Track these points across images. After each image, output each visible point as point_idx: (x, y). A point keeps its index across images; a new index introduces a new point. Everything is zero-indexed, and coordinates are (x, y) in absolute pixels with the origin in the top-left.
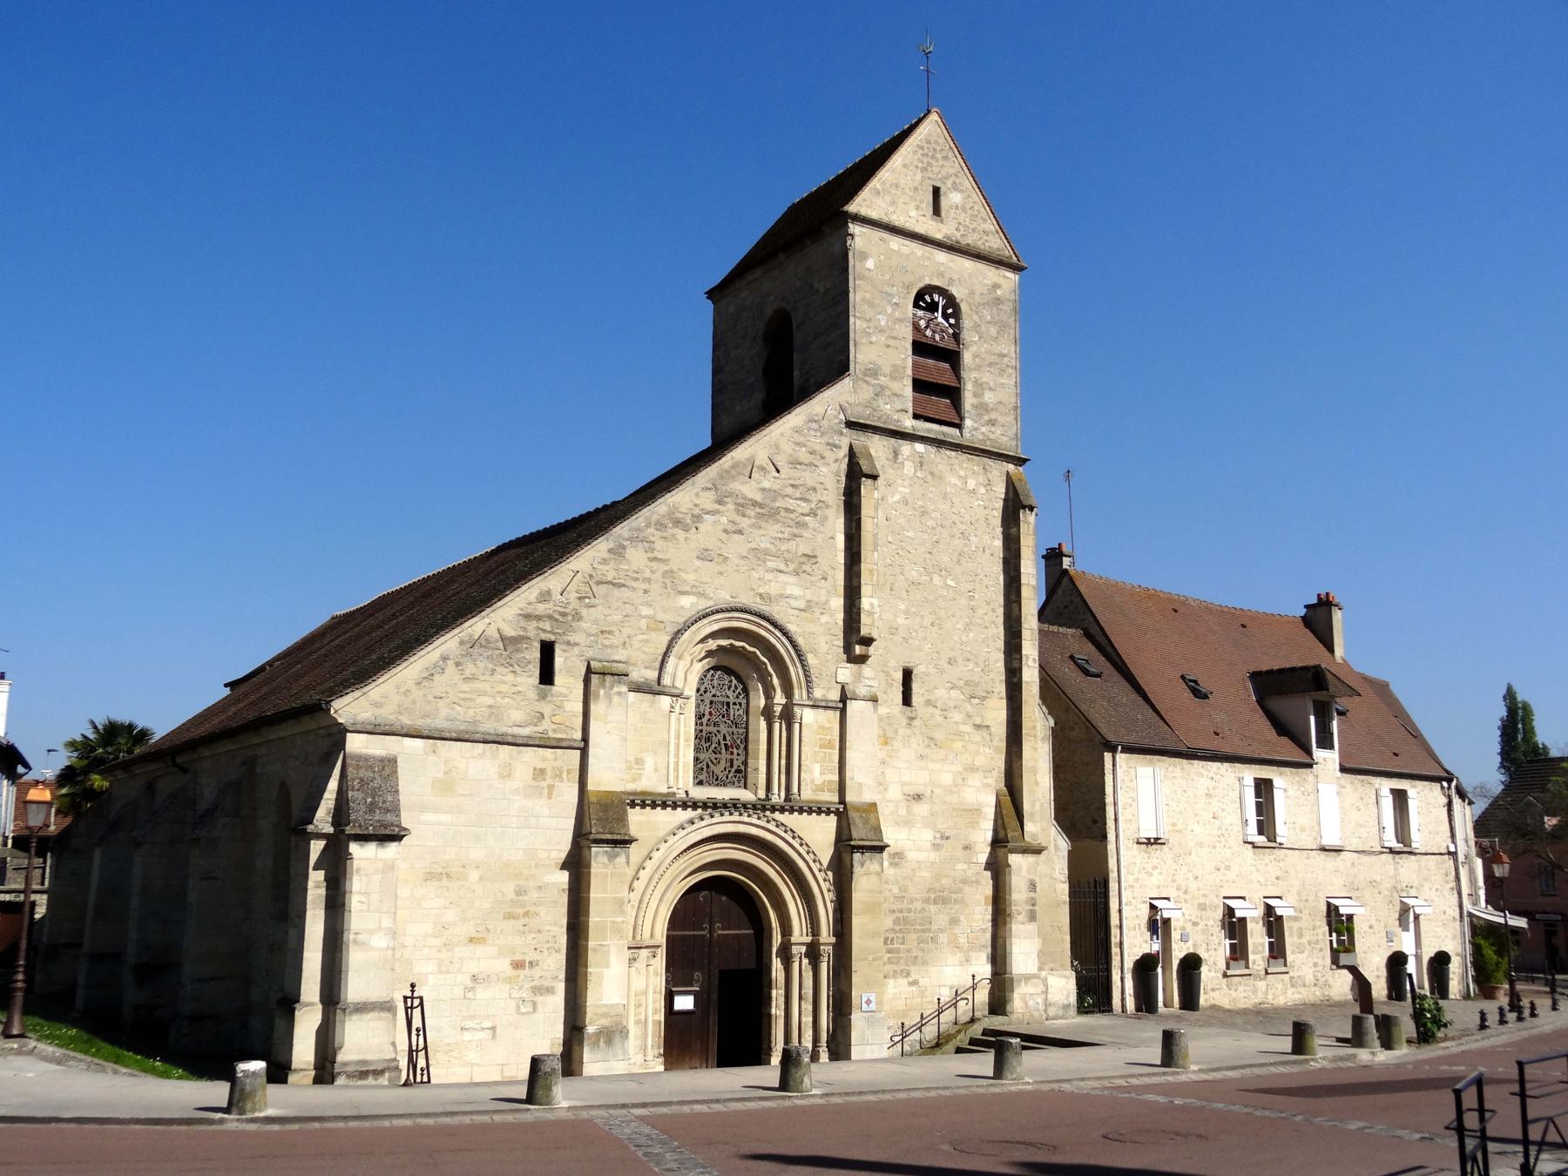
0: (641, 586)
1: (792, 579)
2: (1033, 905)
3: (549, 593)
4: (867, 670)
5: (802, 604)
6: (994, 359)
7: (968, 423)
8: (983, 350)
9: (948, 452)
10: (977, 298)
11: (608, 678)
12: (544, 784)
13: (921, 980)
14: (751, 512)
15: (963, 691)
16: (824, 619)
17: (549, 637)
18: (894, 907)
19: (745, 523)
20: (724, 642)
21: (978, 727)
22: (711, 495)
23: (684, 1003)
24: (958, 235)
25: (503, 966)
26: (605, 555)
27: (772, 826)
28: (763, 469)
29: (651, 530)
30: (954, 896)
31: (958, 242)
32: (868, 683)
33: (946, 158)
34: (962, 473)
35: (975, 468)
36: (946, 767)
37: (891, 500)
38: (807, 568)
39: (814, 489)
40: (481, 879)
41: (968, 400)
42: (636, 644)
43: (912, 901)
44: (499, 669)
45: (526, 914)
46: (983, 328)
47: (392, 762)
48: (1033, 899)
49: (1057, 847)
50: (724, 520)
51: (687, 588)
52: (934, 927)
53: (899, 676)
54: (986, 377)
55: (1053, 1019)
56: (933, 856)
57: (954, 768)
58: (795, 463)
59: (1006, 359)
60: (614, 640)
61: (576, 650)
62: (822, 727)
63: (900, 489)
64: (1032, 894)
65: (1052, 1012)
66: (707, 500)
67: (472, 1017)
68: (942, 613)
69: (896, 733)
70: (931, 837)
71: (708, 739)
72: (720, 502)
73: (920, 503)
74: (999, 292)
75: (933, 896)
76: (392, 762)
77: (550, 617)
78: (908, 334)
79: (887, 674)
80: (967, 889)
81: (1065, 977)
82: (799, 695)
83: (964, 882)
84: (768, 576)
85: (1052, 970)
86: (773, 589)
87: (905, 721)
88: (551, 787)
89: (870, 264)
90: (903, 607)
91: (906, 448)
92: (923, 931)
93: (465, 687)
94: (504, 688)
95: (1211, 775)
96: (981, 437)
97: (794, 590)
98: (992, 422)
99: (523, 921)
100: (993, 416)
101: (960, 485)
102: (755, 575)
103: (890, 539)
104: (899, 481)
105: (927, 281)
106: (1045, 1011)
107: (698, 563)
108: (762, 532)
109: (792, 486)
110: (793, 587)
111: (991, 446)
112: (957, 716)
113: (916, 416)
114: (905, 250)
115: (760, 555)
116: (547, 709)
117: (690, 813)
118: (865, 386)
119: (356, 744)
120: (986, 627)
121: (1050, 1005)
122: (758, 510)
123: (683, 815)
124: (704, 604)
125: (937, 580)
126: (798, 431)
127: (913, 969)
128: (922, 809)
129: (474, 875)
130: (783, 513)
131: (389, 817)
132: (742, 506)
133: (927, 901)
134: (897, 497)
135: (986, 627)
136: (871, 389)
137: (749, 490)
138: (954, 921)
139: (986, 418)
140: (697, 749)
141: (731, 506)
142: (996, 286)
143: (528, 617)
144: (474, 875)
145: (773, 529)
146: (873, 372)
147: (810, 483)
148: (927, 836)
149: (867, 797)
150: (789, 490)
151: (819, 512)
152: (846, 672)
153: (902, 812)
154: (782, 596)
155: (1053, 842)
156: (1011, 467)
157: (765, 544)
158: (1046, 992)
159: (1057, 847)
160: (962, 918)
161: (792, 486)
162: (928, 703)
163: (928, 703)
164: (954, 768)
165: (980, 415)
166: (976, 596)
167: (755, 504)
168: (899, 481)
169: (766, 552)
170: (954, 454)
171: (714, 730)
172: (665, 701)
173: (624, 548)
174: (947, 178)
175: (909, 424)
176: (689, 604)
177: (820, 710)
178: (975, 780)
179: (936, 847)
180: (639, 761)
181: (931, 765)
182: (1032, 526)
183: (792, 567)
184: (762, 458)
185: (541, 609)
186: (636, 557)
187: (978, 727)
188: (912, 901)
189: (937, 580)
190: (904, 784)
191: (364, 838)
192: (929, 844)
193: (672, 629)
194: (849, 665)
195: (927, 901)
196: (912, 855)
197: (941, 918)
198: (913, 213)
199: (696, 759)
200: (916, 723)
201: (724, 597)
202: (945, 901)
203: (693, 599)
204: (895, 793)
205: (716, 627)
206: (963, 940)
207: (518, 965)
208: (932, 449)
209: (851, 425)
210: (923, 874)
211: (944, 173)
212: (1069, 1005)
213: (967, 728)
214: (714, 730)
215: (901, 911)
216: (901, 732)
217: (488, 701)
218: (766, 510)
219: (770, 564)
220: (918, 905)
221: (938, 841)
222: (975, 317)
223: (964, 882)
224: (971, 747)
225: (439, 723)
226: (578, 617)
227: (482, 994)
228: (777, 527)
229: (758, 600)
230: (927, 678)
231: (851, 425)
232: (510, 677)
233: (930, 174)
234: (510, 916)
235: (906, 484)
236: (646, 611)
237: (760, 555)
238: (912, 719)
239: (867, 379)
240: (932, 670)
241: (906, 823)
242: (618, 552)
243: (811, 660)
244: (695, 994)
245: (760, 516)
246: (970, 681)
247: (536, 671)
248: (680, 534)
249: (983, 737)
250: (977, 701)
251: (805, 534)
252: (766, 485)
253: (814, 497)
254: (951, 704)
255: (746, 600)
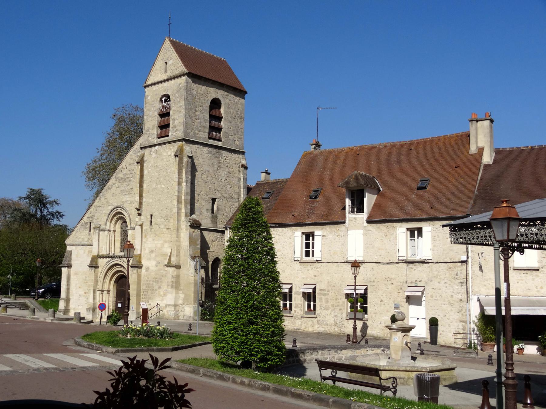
0: (103, 206)
1: (128, 196)
2: (173, 283)
3: (91, 212)
4: (142, 217)
5: (129, 202)
6: (179, 109)
7: (170, 134)
8: (175, 108)
9: (164, 146)
10: (175, 92)
11: (96, 229)
12: (89, 254)
13: (151, 304)
14: (121, 181)
15: (165, 218)
16: (134, 205)
17: (90, 221)
18: (146, 283)
19: (120, 184)
20: (117, 216)
21: (168, 229)
22: (115, 179)
23: (120, 305)
24: (171, 74)
25: (83, 293)
26: (98, 200)
27: (122, 261)
28: (124, 168)
29: (105, 192)
30: (160, 280)
31: (171, 76)
32: (142, 220)
33: (169, 51)
34: (167, 151)
35: (171, 147)
36: (159, 242)
37: (149, 166)
38: (131, 192)
39: (133, 170)
40: (81, 275)
41: (171, 125)
42: (102, 220)
43: (150, 281)
44: (84, 230)
45: (87, 282)
46: (176, 100)
47: (71, 251)
48: (172, 281)
49: (190, 265)
50: (117, 185)
51: (110, 204)
52: (155, 289)
53: (150, 217)
54: (176, 116)
55: (185, 320)
56: (156, 268)
57: (161, 242)
58: (130, 164)
59: (181, 107)
60: (99, 220)
61: (94, 223)
62: (132, 234)
63: (151, 162)
64: (173, 280)
65: (185, 318)
66: (114, 182)
67: (80, 303)
68: (160, 196)
69: (148, 233)
70: (155, 263)
71: (123, 240)
72: (116, 181)
73: (156, 164)
74: (181, 85)
75: (155, 280)
76: (71, 251)
77: (91, 217)
78: (156, 114)
79: (146, 217)
80: (163, 278)
81: (190, 307)
82: (129, 227)
83: (163, 276)
84: (124, 197)
85: (187, 305)
86: (124, 200)
87: (150, 230)
88: (90, 255)
89: (149, 98)
90: (151, 197)
91: (153, 149)
92: (152, 290)
93: (80, 235)
94: (84, 234)
95: (279, 233)
96: (173, 136)
97: (128, 199)
98: (177, 130)
99: (86, 284)
100: (177, 128)
101: (166, 154)
102: (121, 197)
103: (149, 178)
104: (151, 160)
105: (162, 94)
106: (183, 317)
107: (112, 197)
108: (123, 185)
109: (129, 171)
110: (128, 198)
111: (176, 138)
112: (162, 226)
113: (159, 138)
114: (157, 88)
115: (122, 191)
116: (90, 237)
117: (109, 259)
118: (146, 135)
119: (68, 248)
120: (172, 197)
121: (185, 315)
122: (122, 180)
123: (108, 259)
124: (113, 207)
125: (159, 186)
126: (131, 155)
127: (150, 300)
128: (153, 255)
129: (80, 274)
130: (127, 179)
131: (69, 263)
132: (119, 180)
133: (153, 281)
134: (151, 164)
135: (172, 197)
136: (147, 135)
137: (121, 175)
138: (160, 287)
139: (175, 130)
140: (121, 243)
141: (118, 181)
142: (180, 84)
143: (88, 218)
144: (80, 274)
145: (125, 184)
146: (148, 130)
147: (133, 168)
148: (154, 263)
149: (139, 253)
150: (129, 172)
151: (134, 176)
152: (137, 219)
153: (149, 256)
154: (126, 201)
155: (189, 264)
156: (180, 143)
157: (123, 189)
158: (184, 311)
159: (190, 265)
160: (162, 287)
161: (129, 171)
162: (156, 224)
163: (156, 224)
164: (161, 242)
165: (174, 129)
166: (169, 188)
167: (122, 178)
168: (151, 160)
169: (123, 191)
170: (165, 145)
171: (124, 237)
172: (106, 232)
173: (101, 197)
174: (168, 58)
175: (156, 141)
176: (111, 208)
177: (132, 230)
178: (166, 245)
179: (157, 266)
180: (102, 247)
181: (156, 242)
182: (178, 161)
183: (128, 193)
184: (124, 167)
185: (90, 216)
186: (103, 199)
187: (168, 229)
188: (150, 281)
189: (159, 186)
190: (149, 248)
191: (63, 267)
192: (155, 265)
193: (107, 215)
194: (138, 217)
195: (153, 281)
196: (151, 268)
197: (156, 287)
198: (160, 75)
199: (121, 245)
200: (152, 230)
201: (116, 205)
202: (158, 281)
203: (111, 206)
204: (147, 251)
205: (114, 213)
206: (162, 293)
207: (85, 293)
208: (160, 147)
209: (142, 148)
210: (153, 274)
211: (168, 56)
212: (190, 316)
213: (165, 230)
214: (124, 237)
215: (147, 284)
216: (149, 233)
217: (82, 237)
218: (123, 180)
219: (124, 193)
220: (151, 282)
221: (157, 264)
222: (174, 98)
223: (163, 276)
224: (166, 235)
225: (77, 243)
226: (94, 216)
227: (80, 299)
228: (126, 183)
229: (122, 203)
230: (155, 216)
231: (142, 148)
232: (85, 232)
233: (165, 59)
234: (84, 283)
235: (153, 160)
236: (104, 212)
237: (122, 191)
238: (151, 229)
239: (147, 133)
240: (157, 214)
241: (149, 259)
242: (100, 199)
243: (131, 217)
244: (122, 303)
245: (123, 182)
246: (167, 215)
247: (89, 229)
248: (109, 191)
249: (169, 232)
250: (168, 221)
251: (131, 183)
252: (124, 173)
253: (133, 172)
254: (161, 223)
255: (120, 204)
